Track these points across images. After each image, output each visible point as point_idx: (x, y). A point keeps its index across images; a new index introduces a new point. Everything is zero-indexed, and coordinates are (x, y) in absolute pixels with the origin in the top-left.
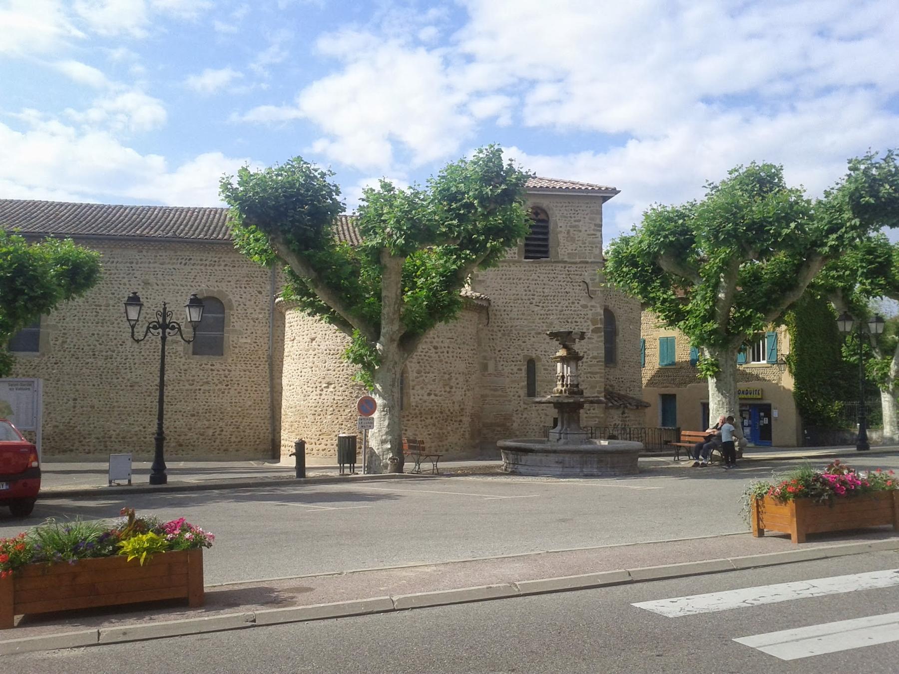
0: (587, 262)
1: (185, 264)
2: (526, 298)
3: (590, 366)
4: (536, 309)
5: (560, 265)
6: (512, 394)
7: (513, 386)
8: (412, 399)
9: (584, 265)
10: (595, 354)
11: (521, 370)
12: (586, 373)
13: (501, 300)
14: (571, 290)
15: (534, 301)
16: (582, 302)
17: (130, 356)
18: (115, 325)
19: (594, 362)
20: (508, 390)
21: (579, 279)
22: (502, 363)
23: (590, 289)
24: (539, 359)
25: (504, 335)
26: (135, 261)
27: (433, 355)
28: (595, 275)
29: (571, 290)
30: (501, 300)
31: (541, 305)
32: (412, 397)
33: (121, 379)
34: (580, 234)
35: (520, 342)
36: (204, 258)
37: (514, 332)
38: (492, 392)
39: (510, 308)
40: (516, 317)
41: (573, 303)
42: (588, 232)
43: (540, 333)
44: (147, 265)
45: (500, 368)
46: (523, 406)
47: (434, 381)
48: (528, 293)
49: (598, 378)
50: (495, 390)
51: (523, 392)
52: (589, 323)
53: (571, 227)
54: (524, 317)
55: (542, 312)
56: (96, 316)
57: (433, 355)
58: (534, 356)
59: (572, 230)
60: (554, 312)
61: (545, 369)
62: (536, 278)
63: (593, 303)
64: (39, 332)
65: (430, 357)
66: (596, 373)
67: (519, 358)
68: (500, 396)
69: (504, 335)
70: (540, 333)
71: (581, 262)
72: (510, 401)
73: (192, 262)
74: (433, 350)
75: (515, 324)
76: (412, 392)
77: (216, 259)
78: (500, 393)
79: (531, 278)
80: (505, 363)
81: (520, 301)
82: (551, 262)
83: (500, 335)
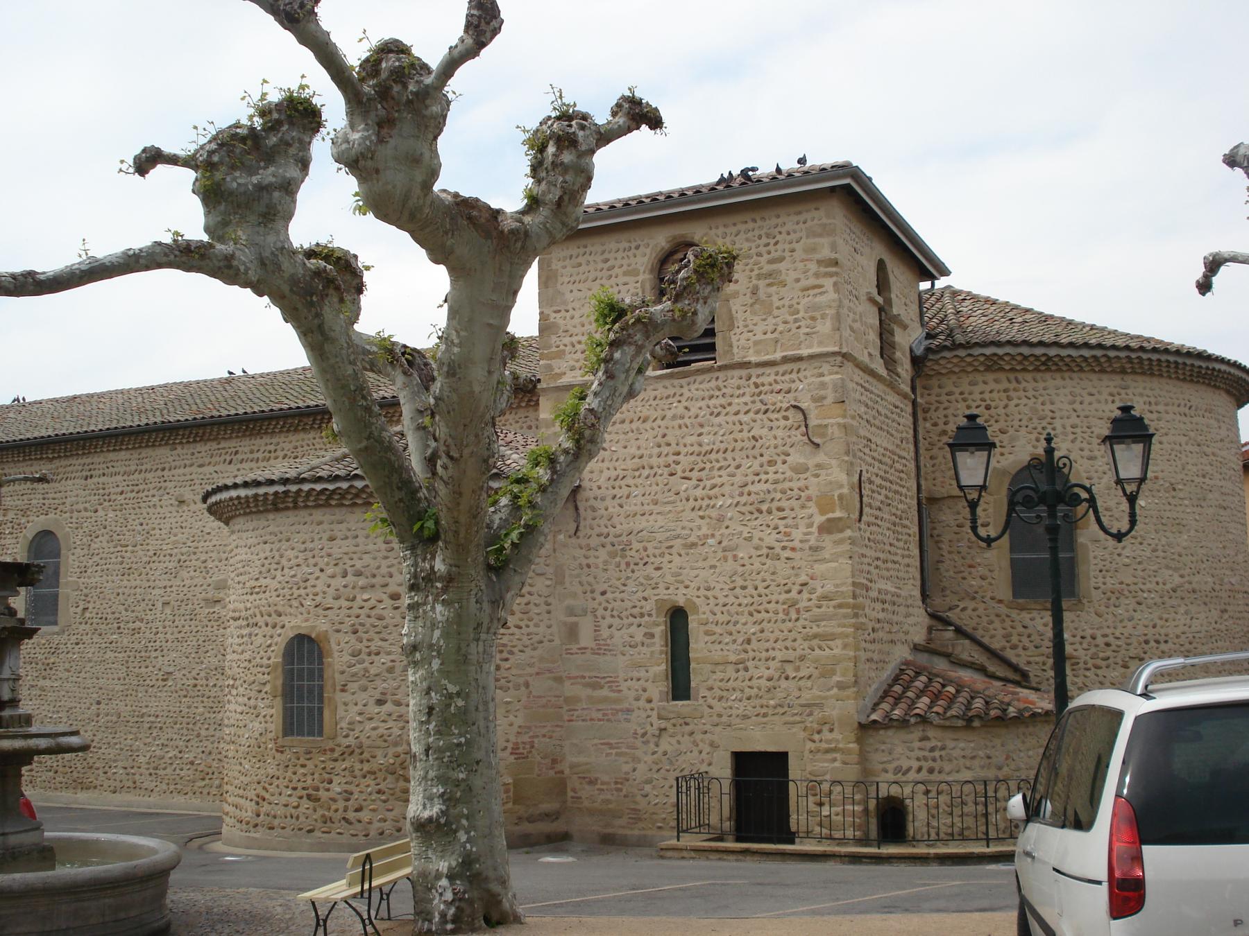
0: (800, 359)
1: (230, 463)
2: (662, 461)
3: (816, 620)
4: (685, 485)
5: (737, 373)
6: (633, 694)
7: (635, 674)
8: (341, 712)
9: (795, 366)
10: (829, 587)
11: (652, 636)
12: (807, 638)
13: (606, 474)
14: (764, 432)
15: (679, 468)
16: (795, 458)
17: (161, 629)
18: (143, 576)
19: (828, 608)
20: (624, 686)
21: (783, 401)
22: (609, 620)
23: (813, 422)
24: (696, 609)
25: (613, 555)
26: (167, 466)
27: (388, 613)
28: (823, 385)
29: (764, 432)
30: (606, 474)
31: (695, 474)
32: (341, 709)
33: (151, 668)
34: (783, 291)
35: (650, 569)
36: (255, 448)
37: (636, 546)
38: (589, 691)
39: (625, 491)
40: (638, 509)
41: (771, 463)
42: (804, 283)
43: (693, 545)
44: (181, 471)
45: (605, 633)
46: (658, 724)
47: (390, 670)
48: (665, 450)
49: (837, 649)
50: (595, 686)
51: (659, 688)
52: (813, 509)
53: (759, 277)
54: (657, 509)
55: (699, 492)
56: (122, 563)
57: (388, 613)
58: (681, 602)
59: (762, 283)
60: (726, 489)
61: (707, 633)
62: (681, 410)
63: (821, 458)
64: (56, 596)
65: (380, 618)
66: (832, 637)
67: (649, 606)
68: (606, 700)
69: (613, 555)
70: (693, 545)
71: (786, 360)
72: (629, 711)
73: (239, 457)
74: (388, 602)
75: (638, 527)
76: (340, 697)
77: (272, 448)
78: (605, 692)
79: (669, 414)
80: (616, 622)
81: (646, 472)
82: (721, 368)
83: (603, 554)
